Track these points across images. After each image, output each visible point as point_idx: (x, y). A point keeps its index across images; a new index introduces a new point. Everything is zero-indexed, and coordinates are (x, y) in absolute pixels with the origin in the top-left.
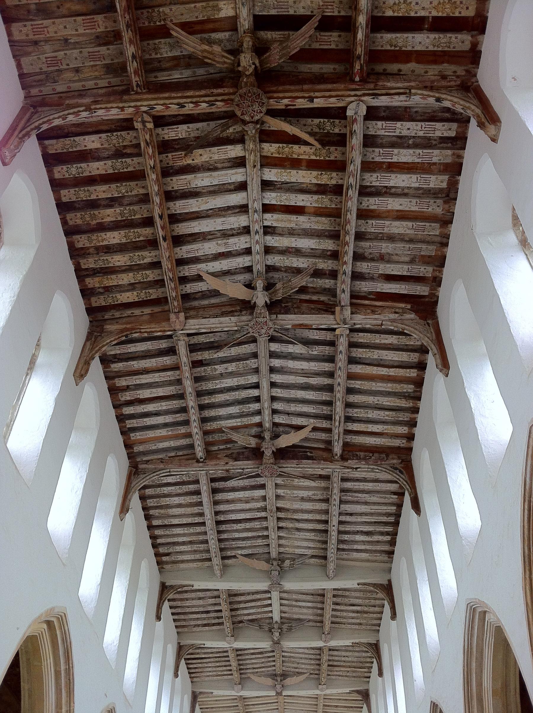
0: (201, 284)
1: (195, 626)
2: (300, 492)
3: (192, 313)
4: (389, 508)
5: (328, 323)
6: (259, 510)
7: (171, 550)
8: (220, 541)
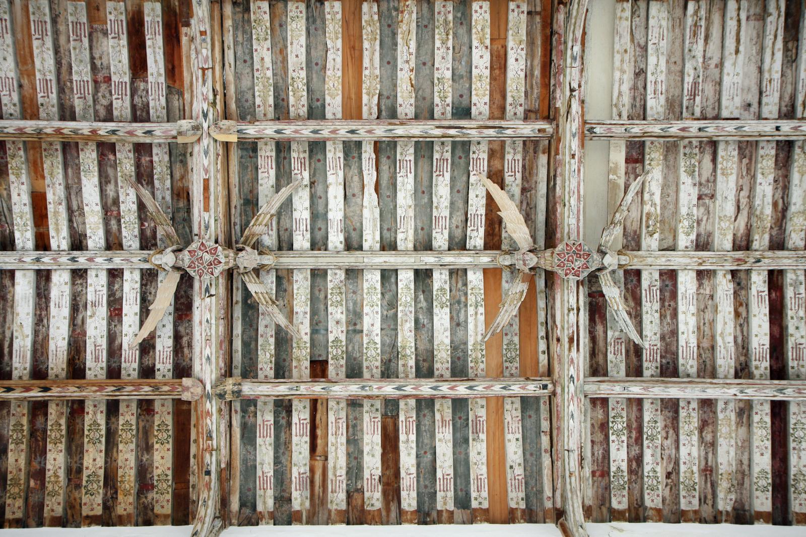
0: (159, 347)
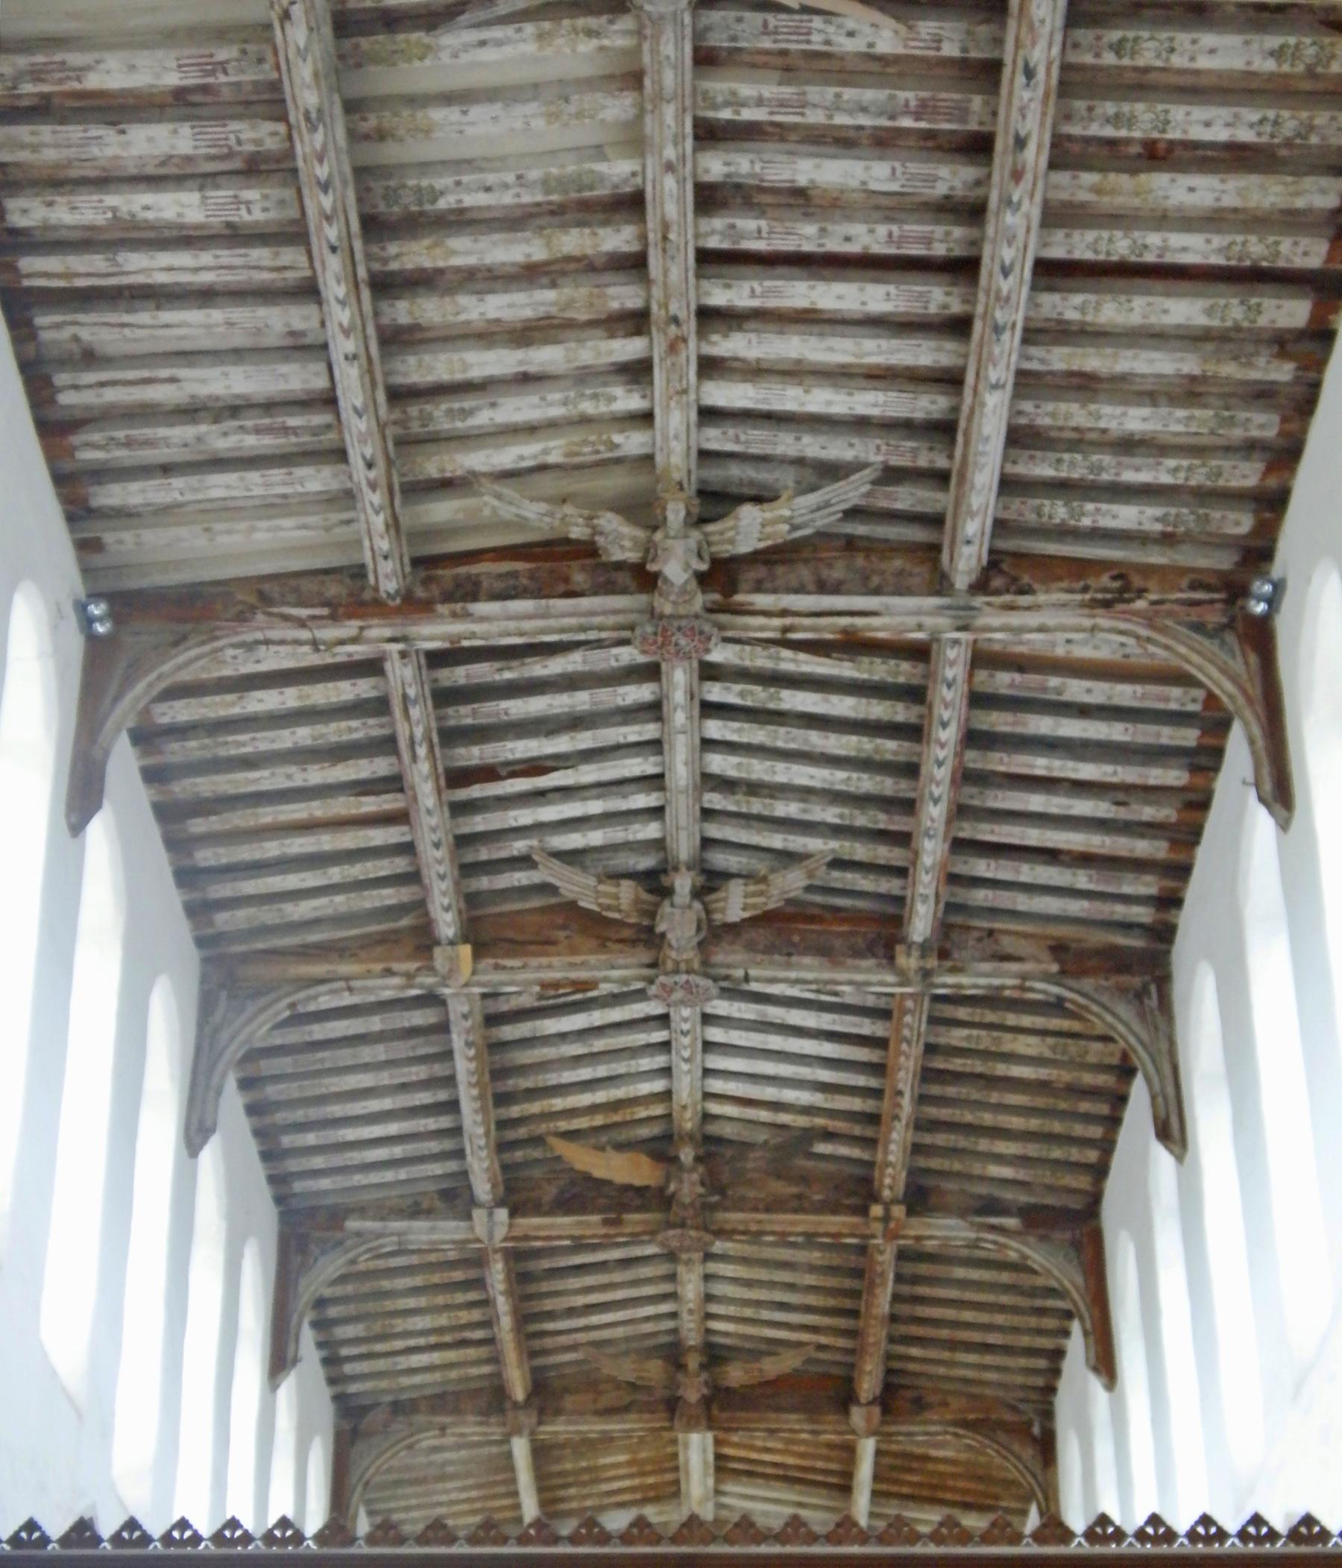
4: (88, 398)
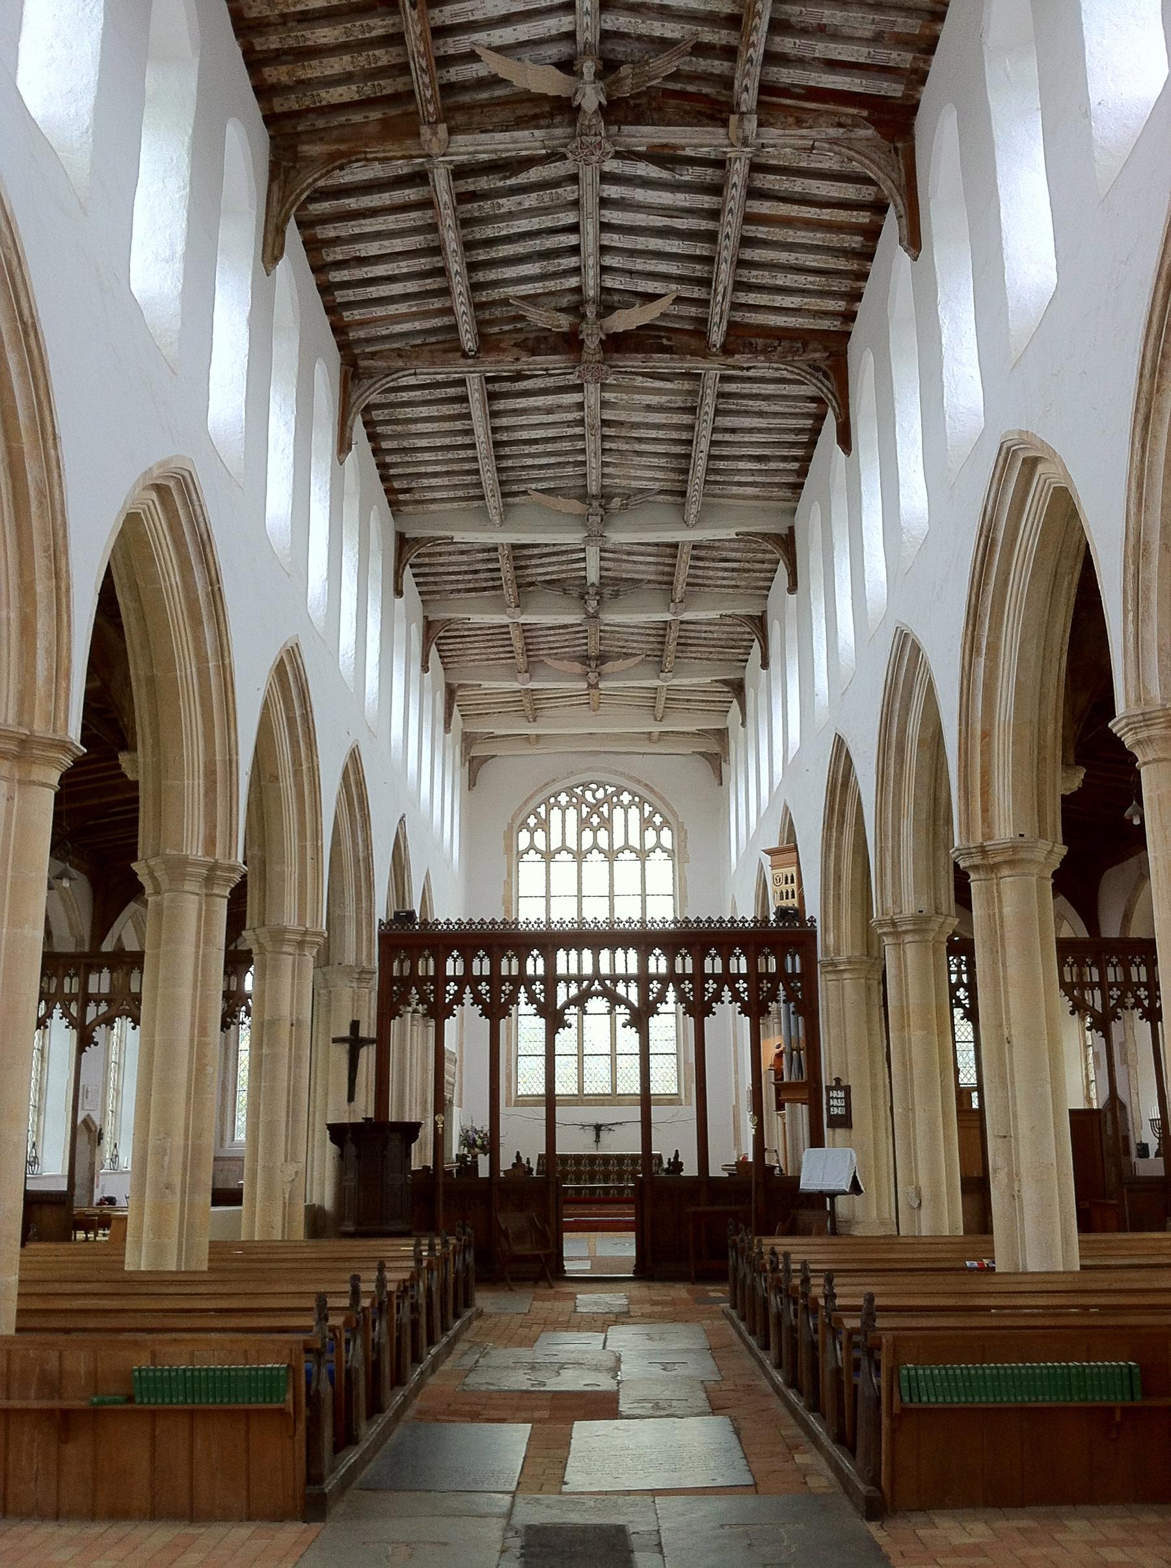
0: (475, 66)
1: (452, 591)
2: (644, 397)
3: (460, 118)
5: (715, 142)
6: (569, 424)
7: (414, 485)
8: (500, 470)
